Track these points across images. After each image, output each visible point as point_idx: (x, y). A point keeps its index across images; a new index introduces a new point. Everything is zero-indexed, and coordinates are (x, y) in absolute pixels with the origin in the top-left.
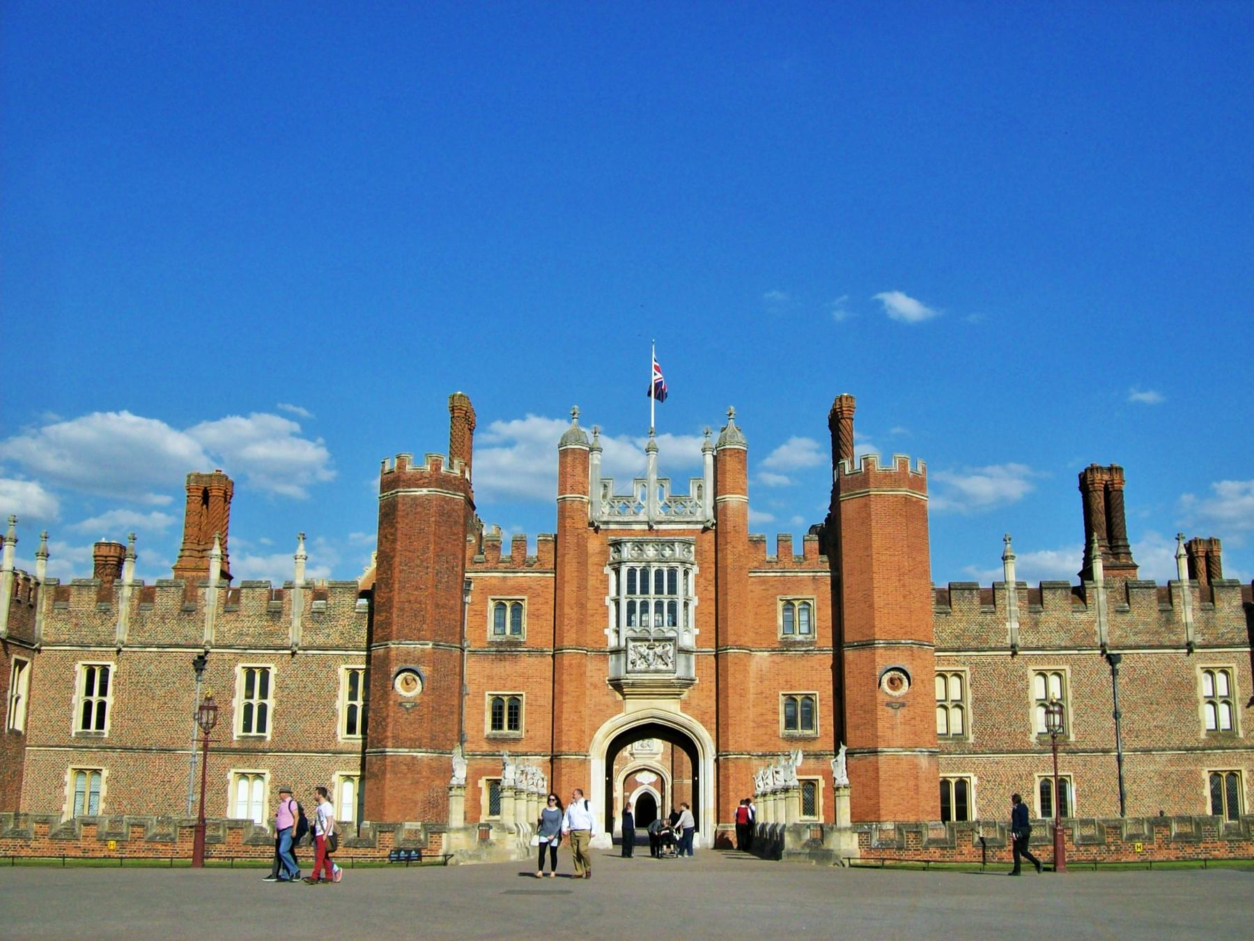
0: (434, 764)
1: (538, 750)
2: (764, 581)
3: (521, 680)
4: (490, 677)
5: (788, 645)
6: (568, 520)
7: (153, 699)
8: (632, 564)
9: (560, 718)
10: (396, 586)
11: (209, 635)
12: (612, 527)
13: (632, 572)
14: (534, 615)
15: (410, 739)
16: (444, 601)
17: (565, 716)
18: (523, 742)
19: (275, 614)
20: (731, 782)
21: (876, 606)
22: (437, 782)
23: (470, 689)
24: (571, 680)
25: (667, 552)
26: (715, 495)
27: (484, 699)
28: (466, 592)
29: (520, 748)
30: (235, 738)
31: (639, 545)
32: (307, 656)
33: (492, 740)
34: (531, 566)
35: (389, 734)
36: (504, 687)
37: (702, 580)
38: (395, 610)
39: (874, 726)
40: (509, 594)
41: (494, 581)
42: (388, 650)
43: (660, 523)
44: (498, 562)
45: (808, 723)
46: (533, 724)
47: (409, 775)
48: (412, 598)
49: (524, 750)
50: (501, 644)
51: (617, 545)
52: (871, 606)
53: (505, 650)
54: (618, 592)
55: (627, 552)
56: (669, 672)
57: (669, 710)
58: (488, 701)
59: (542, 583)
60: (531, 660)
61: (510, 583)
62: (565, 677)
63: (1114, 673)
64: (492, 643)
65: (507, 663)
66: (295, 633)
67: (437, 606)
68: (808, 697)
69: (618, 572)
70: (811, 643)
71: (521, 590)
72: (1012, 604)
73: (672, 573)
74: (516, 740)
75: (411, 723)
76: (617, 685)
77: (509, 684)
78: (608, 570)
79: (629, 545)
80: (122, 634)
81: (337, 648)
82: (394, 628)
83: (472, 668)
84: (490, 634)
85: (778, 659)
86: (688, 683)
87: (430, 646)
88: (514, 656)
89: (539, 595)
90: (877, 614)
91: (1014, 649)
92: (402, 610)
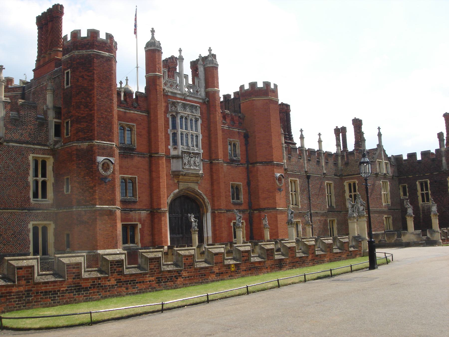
1: (145, 208)
2: (223, 130)
5: (232, 161)
6: (158, 87)
8: (182, 114)
10: (96, 108)
12: (169, 94)
13: (182, 117)
14: (139, 135)
18: (138, 203)
20: (223, 223)
21: (273, 147)
25: (194, 111)
29: (136, 206)
31: (184, 106)
32: (9, 146)
37: (203, 126)
39: (274, 199)
40: (128, 122)
42: (92, 147)
43: (188, 96)
49: (139, 207)
50: (125, 149)
52: (271, 147)
54: (174, 127)
56: (197, 170)
63: (308, 182)
68: (239, 185)
69: (174, 118)
70: (239, 161)
71: (132, 120)
73: (197, 120)
74: (135, 202)
76: (176, 175)
78: (169, 116)
79: (180, 104)
81: (27, 143)
82: (96, 133)
85: (229, 167)
88: (132, 157)
90: (274, 151)
92: (99, 122)
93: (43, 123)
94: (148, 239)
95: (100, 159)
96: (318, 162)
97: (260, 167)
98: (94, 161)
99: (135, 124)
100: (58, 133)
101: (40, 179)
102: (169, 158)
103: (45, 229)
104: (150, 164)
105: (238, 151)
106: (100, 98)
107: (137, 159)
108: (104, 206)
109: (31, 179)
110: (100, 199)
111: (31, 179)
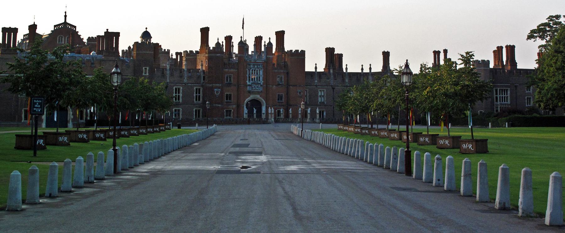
11: (168, 81)
14: (234, 78)
19: (181, 77)
26: (267, 55)
31: (254, 65)
33: (227, 102)
45: (281, 100)
46: (233, 100)
51: (250, 65)
55: (251, 66)
57: (258, 97)
66: (185, 81)
72: (317, 77)
76: (250, 92)
86: (262, 92)
91: (316, 86)
93: (199, 77)
94: (236, 115)
95: (215, 90)
96: (343, 80)
97: (291, 87)
98: (213, 91)
100: (204, 79)
101: (198, 94)
102: (246, 85)
103: (199, 111)
105: (283, 80)
109: (195, 95)
111: (195, 95)
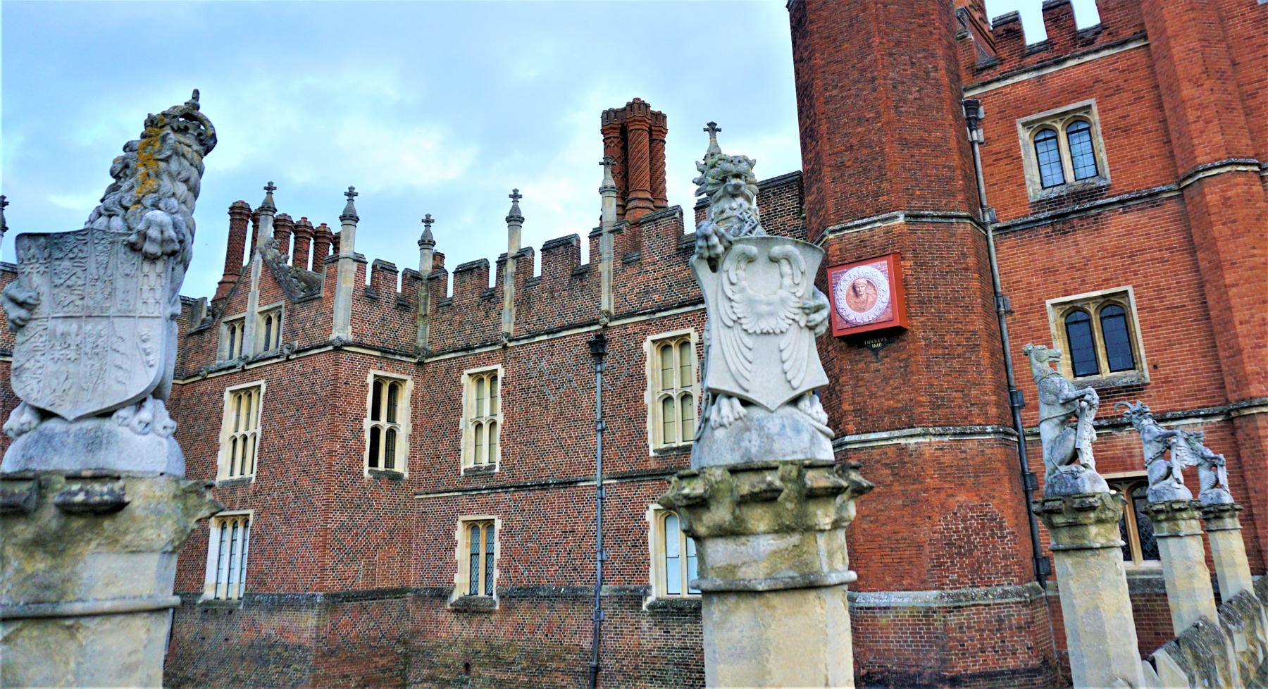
0: (947, 459)
3: (1118, 260)
4: (1049, 271)
7: (546, 408)
9: (1228, 323)
15: (890, 411)
16: (918, 134)
17: (1238, 316)
22: (962, 498)
23: (1014, 301)
24: (1235, 235)
27: (1044, 315)
28: (973, 123)
30: (652, 454)
34: (1091, 42)
35: (846, 407)
36: (1083, 285)
38: (826, 171)
41: (1020, 91)
44: (1023, 57)
47: (897, 487)
48: (854, 142)
50: (1059, 200)
53: (1072, 210)
58: (1055, 320)
59: (1121, 65)
60: (1131, 218)
61: (1055, 84)
62: (1218, 229)
64: (1040, 204)
65: (1079, 236)
67: (904, 143)
71: (1078, 91)
75: (886, 379)
77: (1092, 276)
80: (508, 326)
83: (1014, 262)
84: (1034, 191)
87: (901, 219)
89: (1118, 90)
99: (1091, 101)
104: (1184, 221)
106: (834, 93)
107: (1119, 224)
108: (872, 436)
110: (860, 411)
